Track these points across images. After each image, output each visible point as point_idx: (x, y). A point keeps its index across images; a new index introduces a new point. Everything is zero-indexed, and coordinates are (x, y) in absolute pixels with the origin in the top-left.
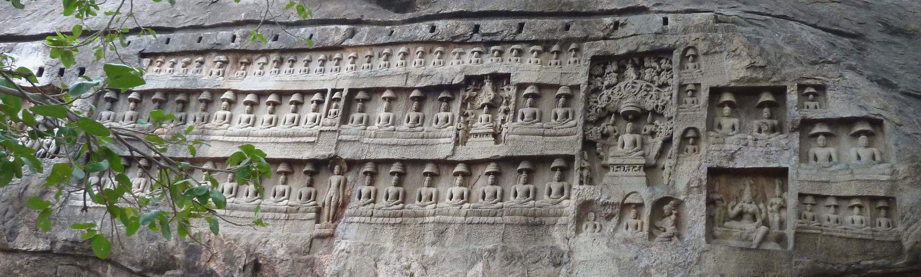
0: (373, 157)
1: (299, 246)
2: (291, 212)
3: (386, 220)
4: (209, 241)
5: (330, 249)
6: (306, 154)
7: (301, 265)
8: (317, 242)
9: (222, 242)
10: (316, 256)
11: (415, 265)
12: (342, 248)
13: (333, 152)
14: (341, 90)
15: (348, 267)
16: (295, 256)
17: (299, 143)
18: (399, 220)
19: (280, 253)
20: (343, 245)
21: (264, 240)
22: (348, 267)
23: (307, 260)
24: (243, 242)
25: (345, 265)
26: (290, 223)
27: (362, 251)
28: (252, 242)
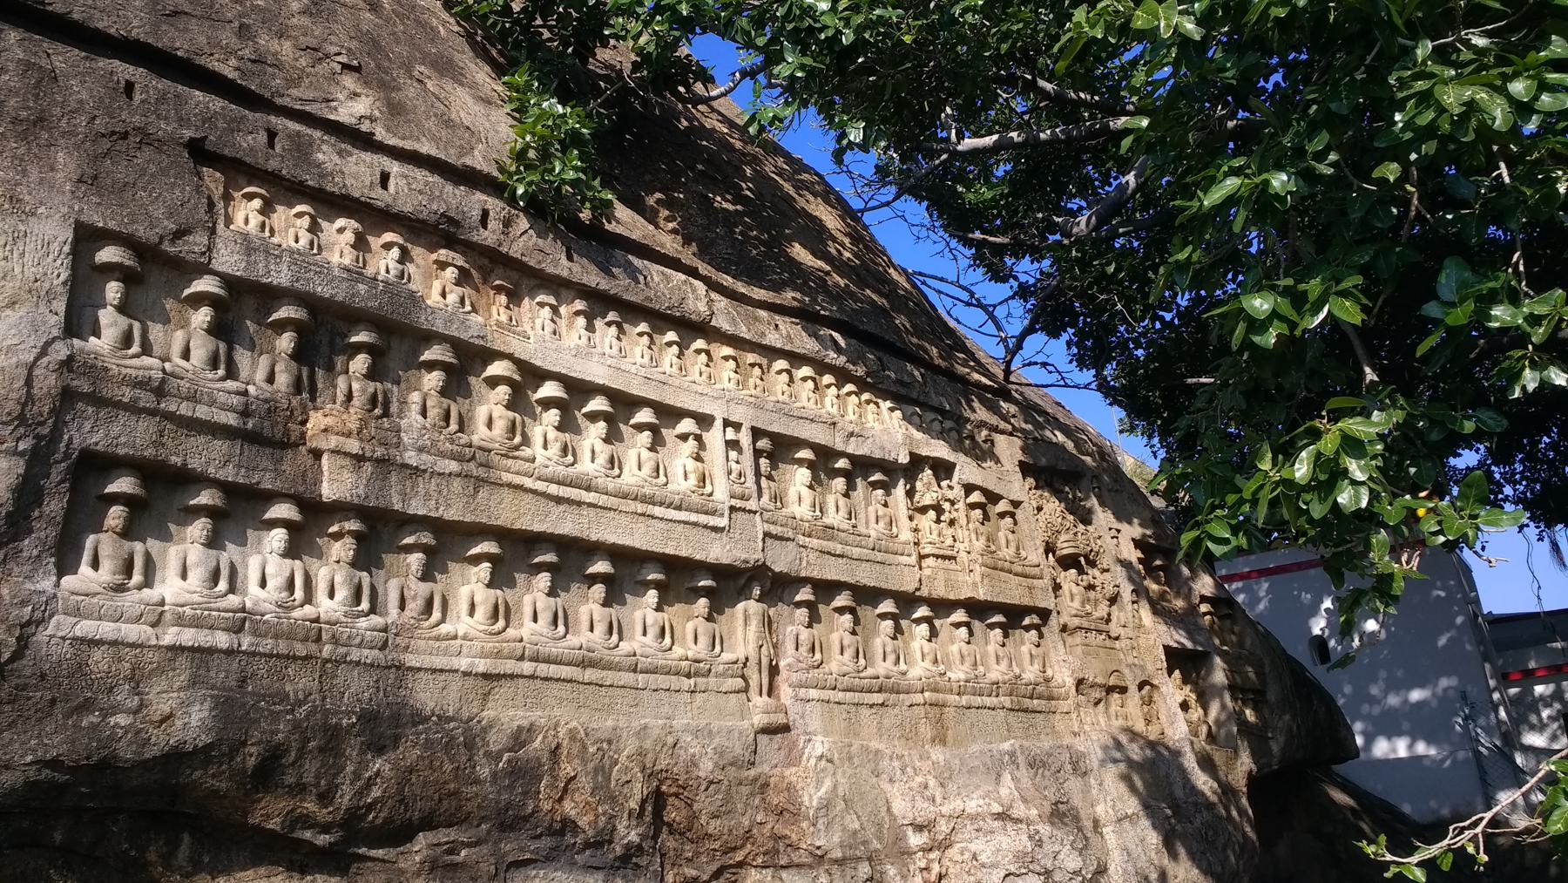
0: (816, 574)
1: (738, 751)
2: (697, 674)
3: (857, 697)
4: (558, 746)
5: (793, 758)
6: (717, 551)
7: (745, 790)
8: (763, 740)
9: (584, 747)
10: (766, 768)
11: (932, 782)
12: (819, 752)
13: (755, 556)
14: (737, 426)
15: (840, 792)
16: (732, 772)
17: (695, 524)
18: (878, 698)
19: (706, 767)
20: (819, 746)
21: (670, 740)
22: (840, 792)
23: (756, 780)
24: (630, 747)
25: (835, 787)
26: (699, 697)
27: (850, 759)
28: (648, 744)
